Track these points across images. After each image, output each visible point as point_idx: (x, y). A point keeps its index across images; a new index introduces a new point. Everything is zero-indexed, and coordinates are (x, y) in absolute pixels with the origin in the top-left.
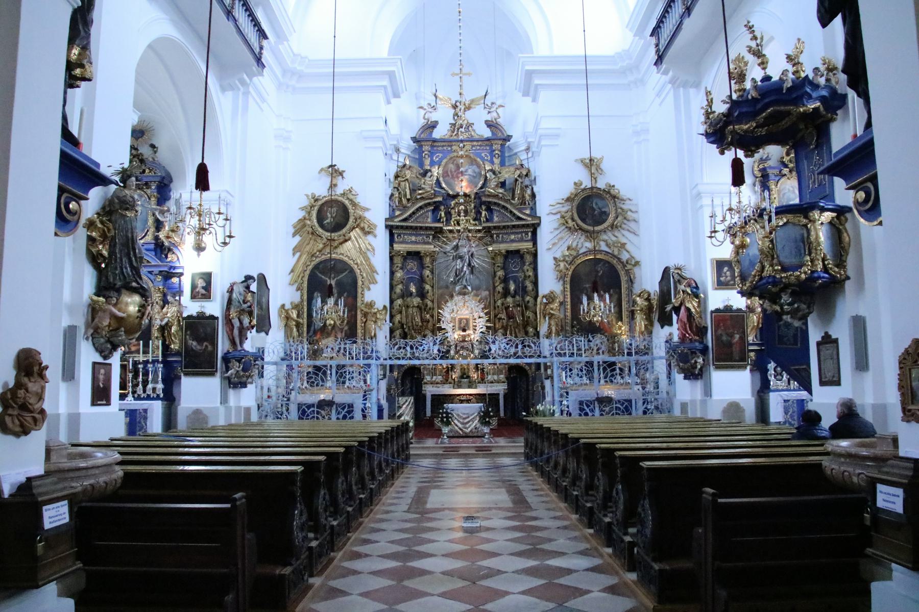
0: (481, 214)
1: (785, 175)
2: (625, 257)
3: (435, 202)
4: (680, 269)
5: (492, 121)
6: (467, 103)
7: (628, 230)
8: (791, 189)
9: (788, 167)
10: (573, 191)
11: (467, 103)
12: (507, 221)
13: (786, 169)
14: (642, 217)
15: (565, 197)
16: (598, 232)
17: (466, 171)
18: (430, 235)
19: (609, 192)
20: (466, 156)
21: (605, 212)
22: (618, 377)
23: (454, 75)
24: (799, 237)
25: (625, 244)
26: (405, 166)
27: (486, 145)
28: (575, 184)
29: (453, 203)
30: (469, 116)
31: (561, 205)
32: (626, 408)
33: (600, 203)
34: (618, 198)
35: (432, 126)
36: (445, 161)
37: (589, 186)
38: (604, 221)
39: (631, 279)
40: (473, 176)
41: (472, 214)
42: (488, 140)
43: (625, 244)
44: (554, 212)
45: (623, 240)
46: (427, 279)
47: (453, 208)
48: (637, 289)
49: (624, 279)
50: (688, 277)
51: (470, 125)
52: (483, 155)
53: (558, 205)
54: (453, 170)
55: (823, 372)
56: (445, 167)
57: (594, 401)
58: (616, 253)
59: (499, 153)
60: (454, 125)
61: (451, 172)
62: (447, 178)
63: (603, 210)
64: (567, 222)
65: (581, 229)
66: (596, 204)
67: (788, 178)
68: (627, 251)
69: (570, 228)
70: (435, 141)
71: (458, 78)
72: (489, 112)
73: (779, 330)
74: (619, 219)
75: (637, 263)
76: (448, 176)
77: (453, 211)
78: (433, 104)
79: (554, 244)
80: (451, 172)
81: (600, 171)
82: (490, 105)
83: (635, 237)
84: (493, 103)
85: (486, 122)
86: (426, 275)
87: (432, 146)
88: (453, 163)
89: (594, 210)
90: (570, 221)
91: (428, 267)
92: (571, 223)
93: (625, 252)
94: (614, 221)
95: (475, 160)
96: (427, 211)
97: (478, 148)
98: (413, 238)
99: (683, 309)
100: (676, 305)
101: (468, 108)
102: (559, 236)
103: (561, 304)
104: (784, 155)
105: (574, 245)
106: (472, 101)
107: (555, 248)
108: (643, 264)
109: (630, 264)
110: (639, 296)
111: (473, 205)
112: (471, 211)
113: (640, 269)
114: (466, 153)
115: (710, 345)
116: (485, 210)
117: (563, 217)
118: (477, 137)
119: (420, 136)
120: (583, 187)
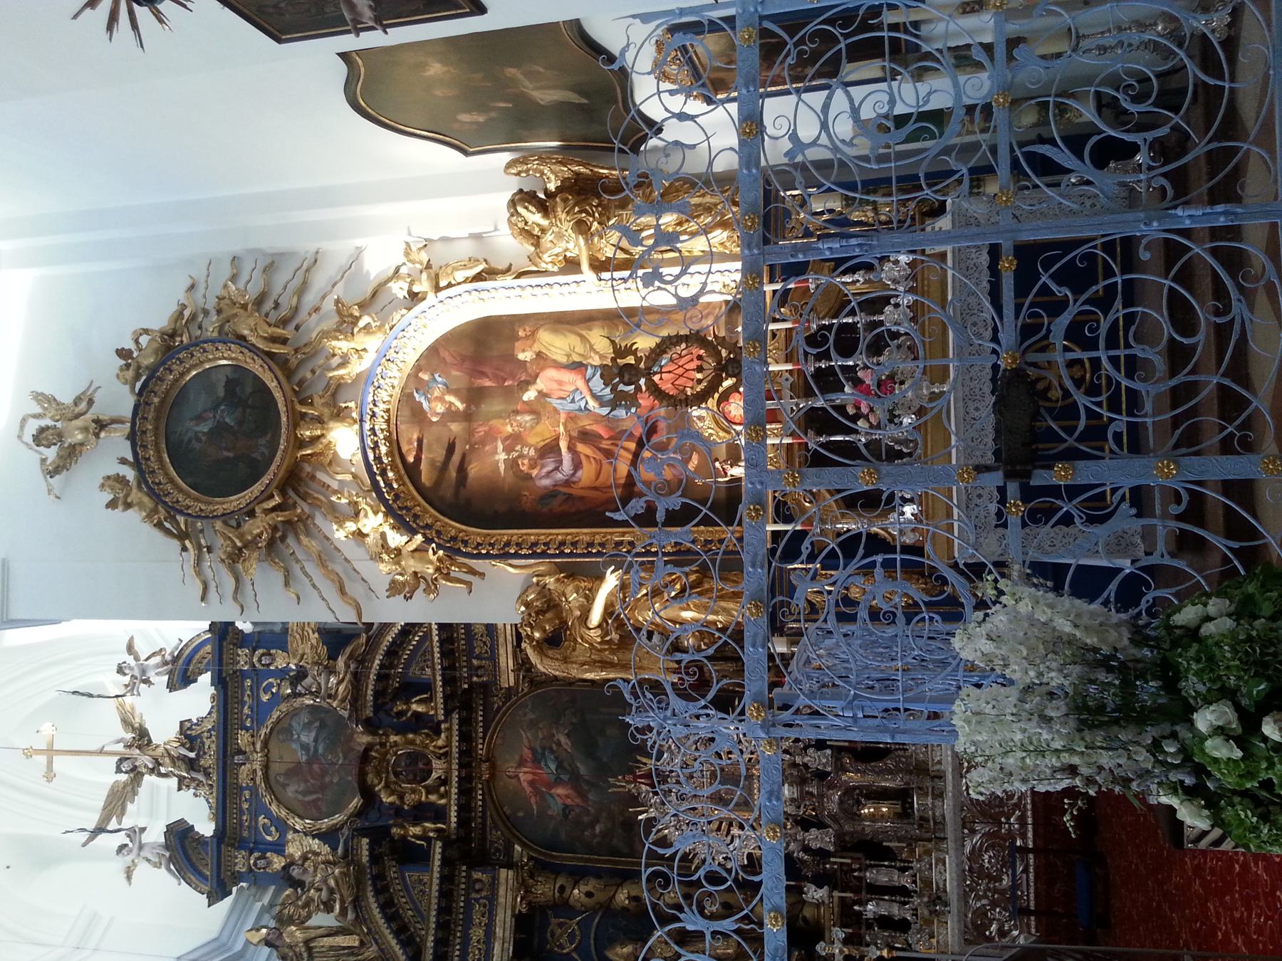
0: (416, 714)
3: (375, 858)
5: (170, 673)
6: (129, 736)
11: (129, 736)
12: (432, 641)
17: (305, 747)
18: (469, 877)
19: (153, 370)
20: (265, 744)
21: (231, 385)
22: (889, 316)
23: (50, 775)
26: (268, 943)
27: (243, 686)
29: (387, 799)
30: (164, 732)
32: (1077, 277)
33: (199, 402)
34: (173, 335)
35: (180, 836)
36: (274, 808)
40: (323, 726)
41: (418, 740)
42: (220, 682)
44: (229, 582)
46: (600, 897)
47: (401, 797)
51: (188, 734)
52: (265, 698)
54: (302, 787)
56: (291, 810)
57: (1028, 494)
59: (261, 651)
60: (181, 780)
61: (305, 793)
62: (324, 809)
63: (221, 392)
66: (199, 418)
70: (220, 834)
71: (59, 762)
72: (147, 682)
74: (246, 332)
76: (314, 801)
77: (410, 799)
78: (121, 838)
79: (342, 591)
80: (305, 793)
81: (83, 406)
82: (127, 679)
84: (120, 670)
85: (172, 687)
86: (584, 899)
87: (240, 844)
88: (284, 786)
91: (562, 889)
92: (257, 526)
94: (253, 349)
95: (279, 720)
96: (403, 878)
97: (246, 710)
98: (477, 933)
101: (142, 737)
103: (571, 572)
106: (127, 723)
110: (536, 240)
111: (393, 738)
112: (412, 742)
114: (258, 746)
116: (408, 702)
118: (214, 715)
119: (206, 878)
120: (130, 474)
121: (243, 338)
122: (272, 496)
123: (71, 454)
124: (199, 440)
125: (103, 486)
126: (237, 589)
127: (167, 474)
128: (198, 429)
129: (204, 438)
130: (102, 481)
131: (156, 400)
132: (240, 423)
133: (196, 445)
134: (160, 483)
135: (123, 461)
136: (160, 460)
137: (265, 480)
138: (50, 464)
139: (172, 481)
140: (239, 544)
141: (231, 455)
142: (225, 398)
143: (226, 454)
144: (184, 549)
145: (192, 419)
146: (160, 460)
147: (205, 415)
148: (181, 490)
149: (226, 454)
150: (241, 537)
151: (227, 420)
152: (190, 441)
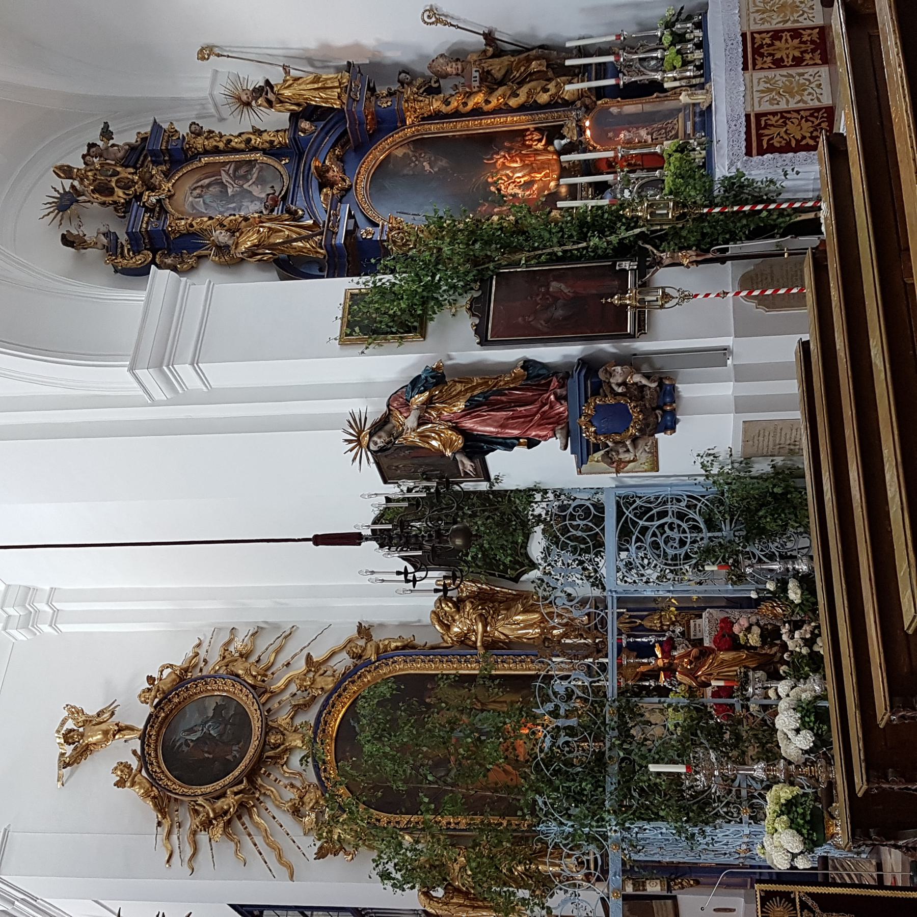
1: (159, 201)
2: (343, 662)
4: (360, 432)
7: (278, 652)
8: (198, 191)
9: (142, 194)
10: (137, 791)
13: (145, 198)
14: (245, 622)
15: (154, 816)
16: (268, 729)
25: (309, 658)
28: (120, 784)
31: (176, 830)
37: (137, 745)
38: (243, 714)
39: (404, 647)
43: (309, 658)
44: (189, 851)
45: (300, 666)
48: (434, 635)
49: (403, 668)
50: (385, 409)
53: (174, 837)
58: (328, 683)
63: (211, 714)
64: (226, 812)
65: (252, 775)
66: (191, 731)
67: (170, 197)
68: (333, 654)
69: (242, 805)
74: (240, 672)
75: (364, 631)
79: (280, 857)
83: (297, 635)
89: (206, 738)
90: (221, 804)
92: (230, 802)
93: (332, 663)
94: (243, 683)
99: (468, 424)
100: (459, 442)
102: (259, 840)
104: (109, 199)
105: (291, 795)
107: (291, 856)
108: (370, 619)
109: (364, 649)
113: (381, 625)
115: (572, 351)
117: (207, 824)
120: (135, 763)
121: (238, 676)
122: (241, 782)
123: (83, 752)
124: (188, 745)
125: (116, 768)
126: (194, 855)
127: (159, 767)
128: (188, 737)
129: (192, 744)
130: (116, 765)
131: (163, 715)
132: (221, 735)
133: (185, 749)
134: (156, 772)
135: (134, 752)
136: (156, 757)
137: (236, 773)
138: (69, 757)
139: (163, 772)
140: (212, 815)
141: (211, 756)
142: (212, 718)
143: (206, 755)
144: (159, 824)
145: (185, 731)
146: (156, 757)
147: (195, 728)
148: (169, 779)
149: (206, 755)
150: (214, 810)
151: (212, 732)
152: (181, 744)
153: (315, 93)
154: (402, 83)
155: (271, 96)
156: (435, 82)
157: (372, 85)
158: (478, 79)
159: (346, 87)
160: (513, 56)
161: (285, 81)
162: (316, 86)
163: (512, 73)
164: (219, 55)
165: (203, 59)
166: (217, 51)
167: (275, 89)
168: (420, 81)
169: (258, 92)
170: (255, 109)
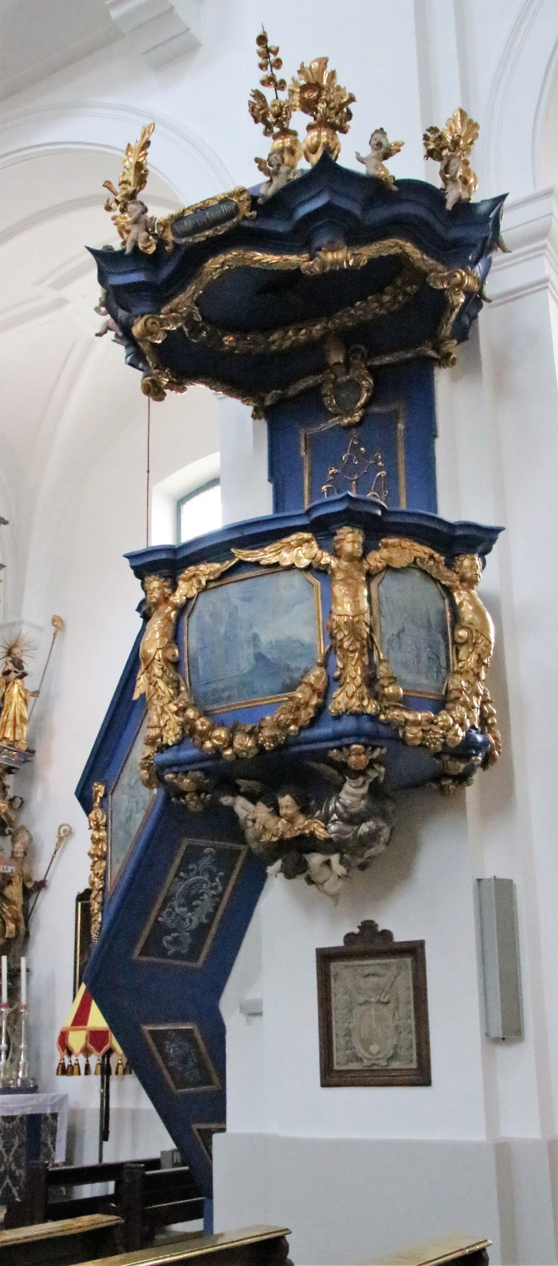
24: (434, 618)
55: (337, 1041)
73: (162, 909)
153: (11, 717)
154: (12, 800)
155: (13, 675)
156: (9, 831)
157: (13, 770)
158: (6, 871)
159: (15, 747)
160: (23, 906)
161: (26, 691)
162: (18, 718)
163: (8, 904)
164: (55, 635)
165: (53, 621)
166: (58, 634)
167: (19, 681)
168: (13, 816)
169: (19, 664)
170: (4, 660)
